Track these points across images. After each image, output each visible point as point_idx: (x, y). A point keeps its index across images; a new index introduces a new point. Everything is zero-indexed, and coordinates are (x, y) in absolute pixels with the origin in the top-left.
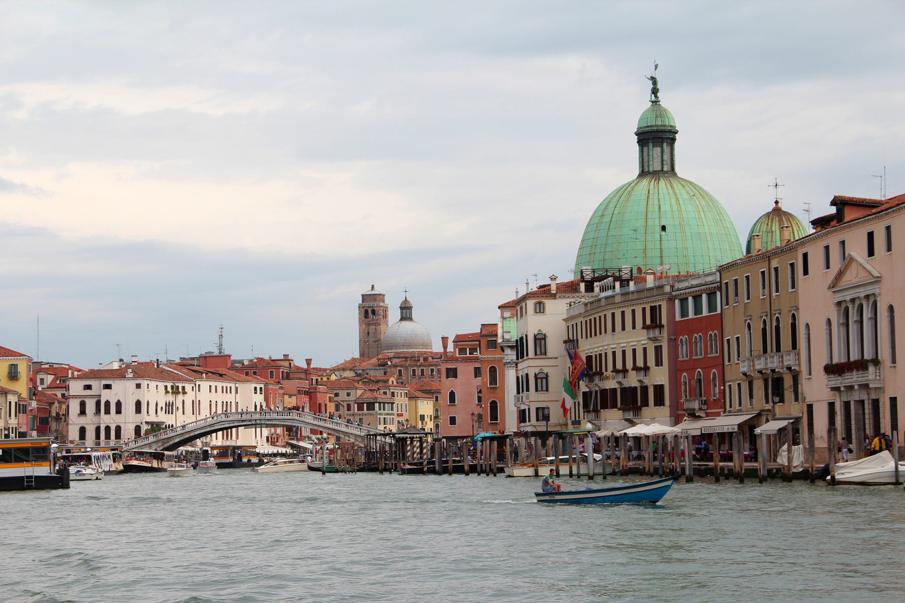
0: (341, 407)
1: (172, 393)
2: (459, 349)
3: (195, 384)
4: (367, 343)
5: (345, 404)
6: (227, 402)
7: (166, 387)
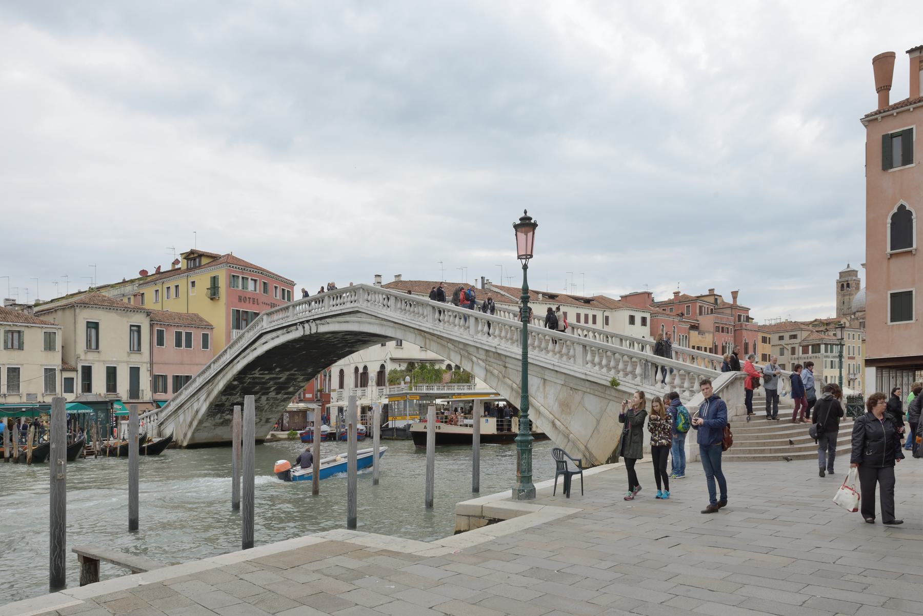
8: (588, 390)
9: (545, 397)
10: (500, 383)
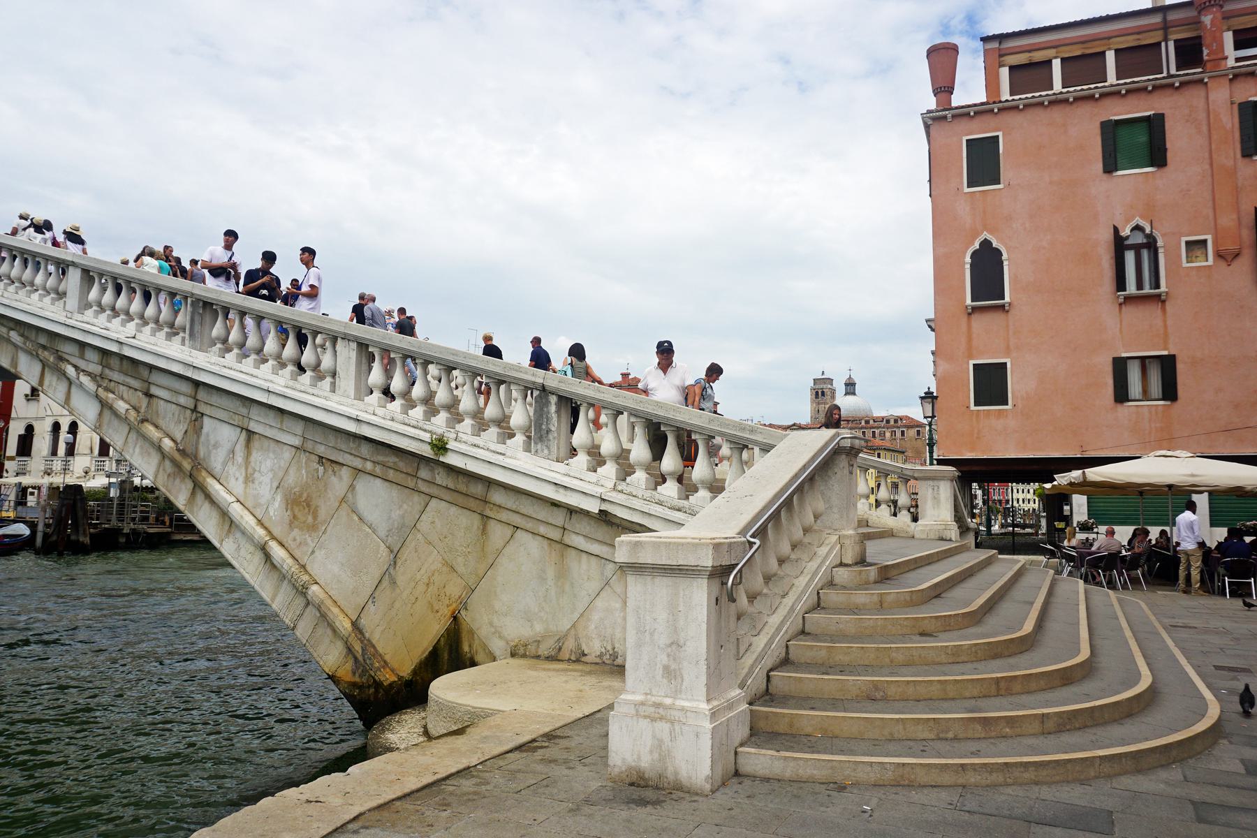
2: (1012, 68)
8: (369, 466)
9: (248, 479)
10: (133, 435)
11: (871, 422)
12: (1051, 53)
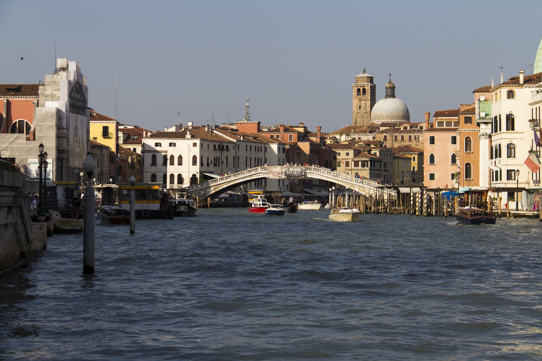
0: (341, 163)
1: (219, 150)
3: (236, 144)
4: (359, 115)
5: (344, 161)
6: (258, 158)
7: (215, 146)
11: (408, 128)
12: (444, 120)
